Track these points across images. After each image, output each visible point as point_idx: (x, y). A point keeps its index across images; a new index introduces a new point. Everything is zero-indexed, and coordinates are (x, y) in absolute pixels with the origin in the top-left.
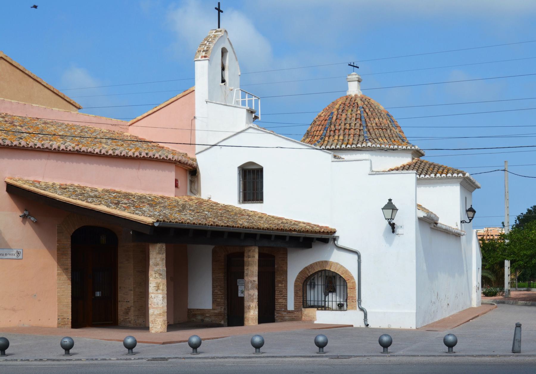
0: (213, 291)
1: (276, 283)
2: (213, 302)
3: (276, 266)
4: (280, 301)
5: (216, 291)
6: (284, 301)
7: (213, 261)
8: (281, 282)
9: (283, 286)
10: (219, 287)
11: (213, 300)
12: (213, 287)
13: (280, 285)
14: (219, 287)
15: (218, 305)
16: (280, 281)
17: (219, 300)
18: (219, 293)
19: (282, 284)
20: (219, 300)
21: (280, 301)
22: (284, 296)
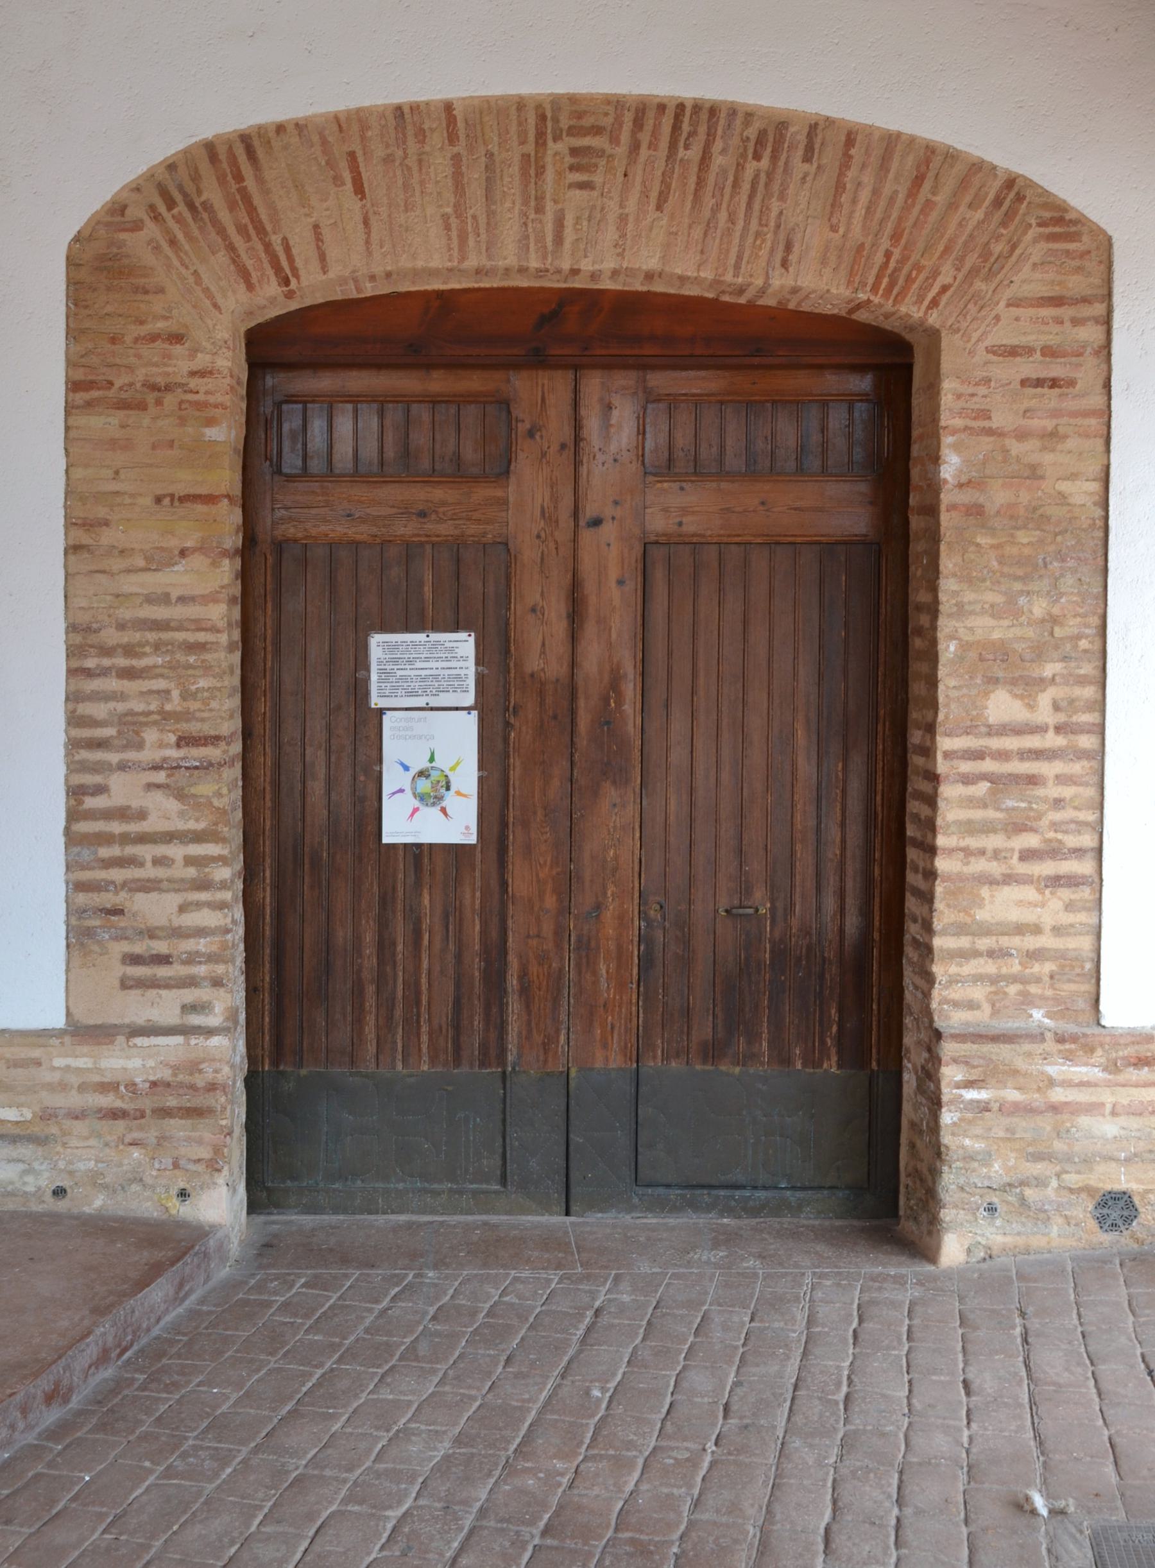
0: (75, 793)
1: (950, 685)
2: (81, 938)
3: (951, 466)
4: (1003, 905)
5: (123, 790)
6: (1052, 909)
7: (73, 386)
8: (1006, 666)
9: (1044, 713)
10: (157, 744)
11: (73, 911)
12: (84, 741)
13: (1002, 706)
14: (157, 744)
15: (147, 968)
16: (1002, 652)
17: (157, 908)
18: (164, 812)
19: (1027, 686)
20: (157, 908)
21: (1003, 905)
22: (1054, 852)
